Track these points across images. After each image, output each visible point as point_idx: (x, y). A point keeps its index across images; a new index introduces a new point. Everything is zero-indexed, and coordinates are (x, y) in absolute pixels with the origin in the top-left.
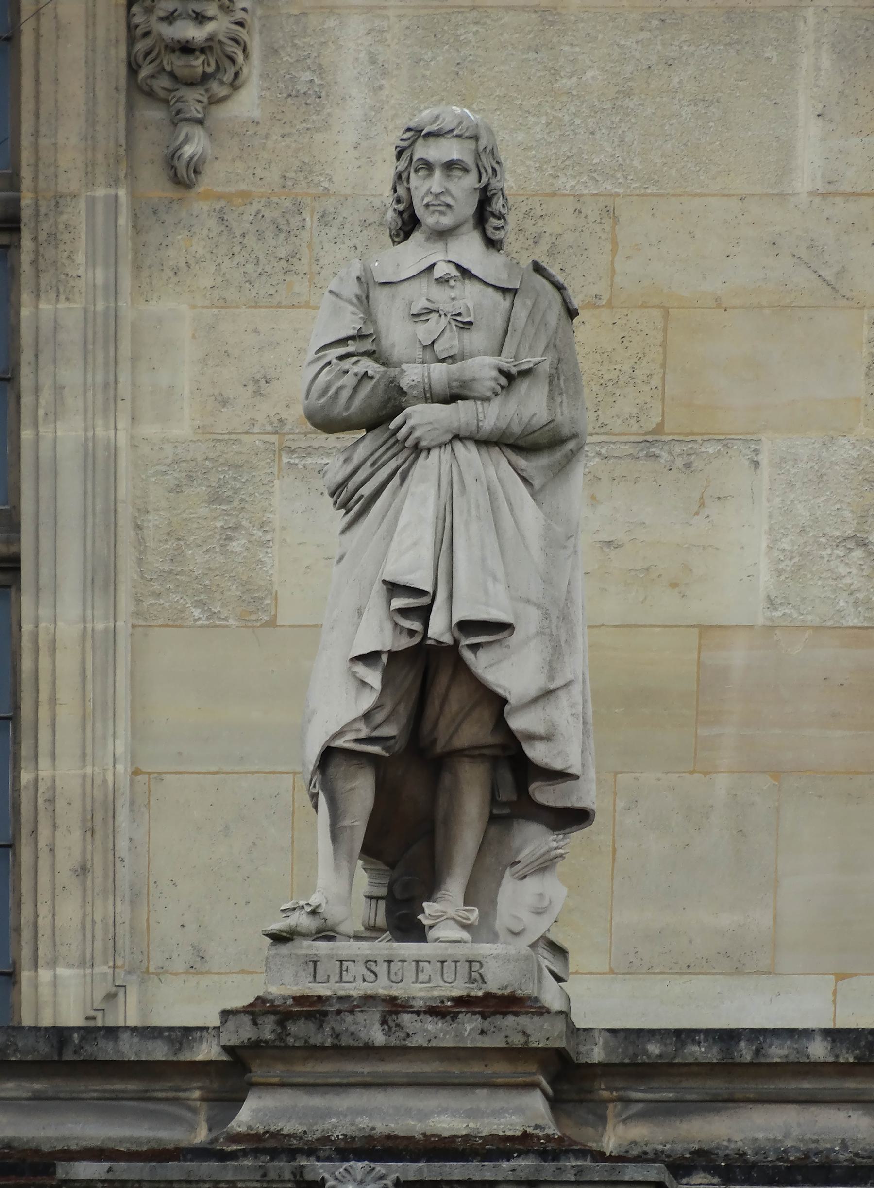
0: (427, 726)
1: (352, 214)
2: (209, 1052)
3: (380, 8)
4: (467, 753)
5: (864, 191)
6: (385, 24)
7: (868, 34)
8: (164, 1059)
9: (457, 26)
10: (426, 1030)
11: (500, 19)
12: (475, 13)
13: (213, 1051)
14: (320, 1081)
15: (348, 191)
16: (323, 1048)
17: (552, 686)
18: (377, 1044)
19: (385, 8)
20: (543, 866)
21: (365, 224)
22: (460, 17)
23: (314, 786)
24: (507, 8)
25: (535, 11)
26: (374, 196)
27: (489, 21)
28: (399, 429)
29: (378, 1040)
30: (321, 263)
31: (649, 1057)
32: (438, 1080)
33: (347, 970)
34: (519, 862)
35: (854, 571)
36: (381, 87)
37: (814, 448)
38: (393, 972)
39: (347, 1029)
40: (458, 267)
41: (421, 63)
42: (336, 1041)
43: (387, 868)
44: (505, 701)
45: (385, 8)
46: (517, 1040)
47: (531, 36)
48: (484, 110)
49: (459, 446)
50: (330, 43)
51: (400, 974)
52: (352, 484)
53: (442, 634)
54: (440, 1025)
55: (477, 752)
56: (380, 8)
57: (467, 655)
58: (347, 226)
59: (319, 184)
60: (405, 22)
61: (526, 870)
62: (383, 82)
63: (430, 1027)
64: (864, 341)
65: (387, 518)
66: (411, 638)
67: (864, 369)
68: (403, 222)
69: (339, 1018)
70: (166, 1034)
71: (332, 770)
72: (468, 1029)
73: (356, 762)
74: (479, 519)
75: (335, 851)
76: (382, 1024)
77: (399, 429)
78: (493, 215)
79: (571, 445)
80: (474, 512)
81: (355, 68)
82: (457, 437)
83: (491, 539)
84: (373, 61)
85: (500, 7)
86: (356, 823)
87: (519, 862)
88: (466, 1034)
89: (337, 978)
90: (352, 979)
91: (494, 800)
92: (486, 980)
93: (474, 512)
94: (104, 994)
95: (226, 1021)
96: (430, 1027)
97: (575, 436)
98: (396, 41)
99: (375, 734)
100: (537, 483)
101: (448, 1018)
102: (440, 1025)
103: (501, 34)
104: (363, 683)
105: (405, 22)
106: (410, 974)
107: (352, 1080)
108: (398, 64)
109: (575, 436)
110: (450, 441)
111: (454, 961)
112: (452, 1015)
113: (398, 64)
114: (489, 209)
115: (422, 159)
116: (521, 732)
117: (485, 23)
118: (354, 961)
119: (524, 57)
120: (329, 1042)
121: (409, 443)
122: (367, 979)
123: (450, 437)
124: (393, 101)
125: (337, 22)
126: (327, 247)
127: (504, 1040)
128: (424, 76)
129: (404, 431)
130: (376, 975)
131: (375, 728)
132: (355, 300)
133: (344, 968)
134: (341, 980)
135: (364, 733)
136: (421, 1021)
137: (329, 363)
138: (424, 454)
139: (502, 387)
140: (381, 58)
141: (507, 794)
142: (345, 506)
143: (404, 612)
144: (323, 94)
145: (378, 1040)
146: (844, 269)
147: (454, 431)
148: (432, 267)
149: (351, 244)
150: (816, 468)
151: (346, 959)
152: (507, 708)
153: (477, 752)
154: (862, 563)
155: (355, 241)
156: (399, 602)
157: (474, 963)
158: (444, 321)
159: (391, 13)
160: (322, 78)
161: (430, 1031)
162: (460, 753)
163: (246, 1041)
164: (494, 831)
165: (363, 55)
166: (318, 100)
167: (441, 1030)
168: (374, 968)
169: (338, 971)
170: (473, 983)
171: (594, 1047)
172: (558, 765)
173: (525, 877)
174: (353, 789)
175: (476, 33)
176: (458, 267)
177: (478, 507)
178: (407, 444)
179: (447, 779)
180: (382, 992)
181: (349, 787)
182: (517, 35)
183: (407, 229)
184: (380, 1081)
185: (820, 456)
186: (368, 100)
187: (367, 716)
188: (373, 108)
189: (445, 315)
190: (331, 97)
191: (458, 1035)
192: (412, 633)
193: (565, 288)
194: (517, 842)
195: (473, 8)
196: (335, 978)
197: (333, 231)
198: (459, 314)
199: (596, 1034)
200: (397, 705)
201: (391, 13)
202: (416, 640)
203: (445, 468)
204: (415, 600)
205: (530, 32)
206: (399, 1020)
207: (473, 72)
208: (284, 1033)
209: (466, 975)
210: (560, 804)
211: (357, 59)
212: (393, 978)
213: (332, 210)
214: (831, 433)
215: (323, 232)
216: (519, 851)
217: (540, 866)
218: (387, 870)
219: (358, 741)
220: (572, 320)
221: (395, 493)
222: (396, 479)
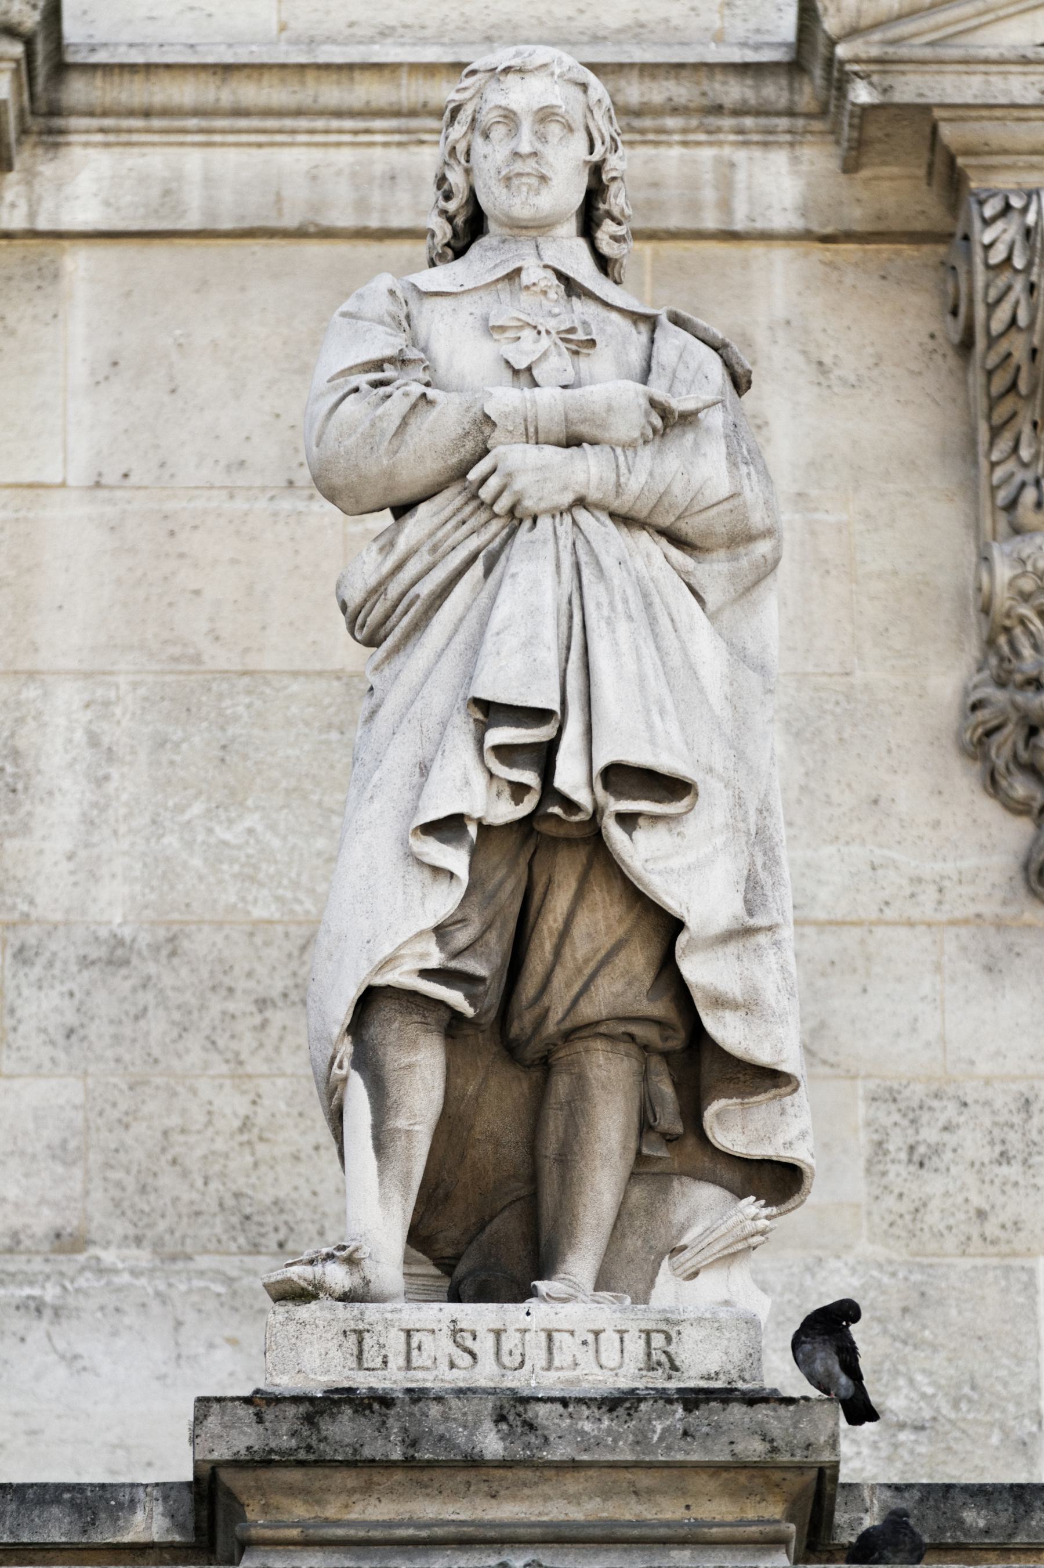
0: (529, 987)
1: (65, 948)
2: (148, 1528)
3: (104, 673)
4: (602, 1029)
5: (848, 919)
6: (112, 694)
7: (838, 710)
8: (63, 1539)
9: (220, 696)
10: (582, 1433)
11: (285, 688)
12: (246, 680)
13: (155, 1528)
14: (376, 1534)
15: (59, 916)
16: (389, 1465)
17: (752, 922)
18: (488, 1456)
19: (111, 673)
20: (731, 1250)
21: (85, 962)
22: (225, 686)
23: (340, 1067)
24: (295, 674)
25: (339, 678)
26: (99, 924)
27: (268, 691)
28: (484, 481)
29: (490, 1449)
30: (19, 1013)
31: (967, 1532)
32: (598, 1532)
33: (419, 1348)
34: (684, 1248)
35: (866, 1451)
36: (107, 778)
37: (792, 1275)
38: (505, 1347)
39: (431, 1431)
40: (561, 276)
41: (169, 746)
42: (411, 1452)
43: (437, 1272)
44: (677, 926)
45: (111, 673)
46: (754, 1449)
47: (332, 710)
48: (264, 808)
49: (583, 516)
50: (29, 720)
51: (517, 1353)
52: (394, 590)
53: (576, 788)
54: (606, 1423)
55: (621, 1028)
56: (104, 673)
57: (615, 833)
58: (58, 965)
59: (14, 907)
60: (142, 691)
61: (699, 1258)
62: (111, 770)
63: (587, 1426)
64: (861, 1123)
65: (460, 638)
66: (517, 804)
67: (862, 1163)
68: (455, 234)
69: (416, 1409)
70: (67, 1496)
71: (374, 1031)
72: (659, 1428)
73: (417, 1018)
74: (630, 618)
75: (381, 1172)
76: (497, 1422)
77: (484, 481)
78: (609, 215)
79: (763, 548)
80: (620, 606)
81: (66, 751)
82: (581, 502)
83: (649, 651)
84: (94, 740)
85: (284, 672)
86: (417, 1128)
87: (684, 1248)
88: (656, 1438)
89: (401, 1361)
90: (429, 1363)
91: (645, 1125)
92: (677, 1363)
93: (620, 606)
94: (514, 106)
95: (205, 1417)
96: (587, 1426)
97: (768, 533)
98: (128, 716)
99: (454, 964)
100: (712, 598)
101: (621, 1411)
102: (606, 1423)
103: (288, 707)
104: (436, 871)
105: (142, 691)
106: (537, 1356)
107: (439, 1532)
108: (132, 747)
109: (768, 533)
110: (570, 509)
111: (619, 1331)
112: (628, 1405)
113: (132, 747)
114: (601, 206)
115: (500, 107)
116: (703, 989)
117: (262, 693)
118: (433, 1331)
119: (324, 737)
120: (397, 1455)
121: (501, 506)
122: (458, 1362)
123: (568, 498)
124: (124, 797)
125: (40, 692)
126: (26, 992)
127: (727, 1449)
128: (172, 763)
129: (493, 483)
130: (473, 1355)
131: (456, 955)
132: (387, 319)
133: (414, 1344)
134: (409, 1365)
135: (436, 959)
136: (571, 1416)
137: (356, 390)
138: (527, 524)
139: (655, 431)
140: (106, 740)
141: (669, 1119)
142: (372, 641)
143: (506, 753)
144: (20, 786)
145: (490, 1449)
146: (823, 1025)
147: (577, 488)
148: (518, 271)
149: (65, 989)
150: (797, 1301)
151: (417, 1326)
152: (682, 940)
153: (621, 1028)
154: (876, 1438)
155: (70, 985)
156: (501, 735)
157: (654, 1335)
158: (545, 342)
159: (121, 680)
160: (17, 766)
161: (587, 1433)
162: (588, 1030)
163: (243, 1452)
164: (638, 1193)
165: (79, 736)
166: (11, 795)
167: (609, 1431)
168: (469, 1343)
169: (402, 1347)
170: (653, 1369)
171: (862, 1515)
172: (763, 1056)
173: (696, 1274)
174: (410, 1066)
175: (249, 706)
176: (561, 276)
177: (626, 601)
178: (497, 508)
179: (561, 1085)
180: (483, 1383)
181: (405, 1061)
182: (311, 709)
183: (459, 244)
184: (492, 1533)
185: (801, 1285)
186: (88, 795)
187: (441, 932)
188: (95, 805)
189: (548, 332)
190: (31, 791)
191: (641, 1440)
192: (519, 790)
193: (726, 346)
194: (679, 1215)
195: (244, 673)
196: (397, 1361)
197: (37, 971)
198: (572, 330)
199: (866, 1493)
200: (488, 927)
201: (121, 680)
202: (528, 805)
203: (565, 542)
204: (530, 732)
205: (330, 705)
206: (530, 1414)
207: (245, 757)
208: (314, 1437)
209: (642, 1356)
210: (757, 1152)
211: (70, 741)
212: (506, 1359)
213: (33, 941)
214: (819, 1253)
215: (21, 974)
216: (683, 1229)
217: (726, 1252)
218: (438, 1277)
219: (426, 974)
220: (740, 396)
221: (476, 593)
222: (478, 568)
